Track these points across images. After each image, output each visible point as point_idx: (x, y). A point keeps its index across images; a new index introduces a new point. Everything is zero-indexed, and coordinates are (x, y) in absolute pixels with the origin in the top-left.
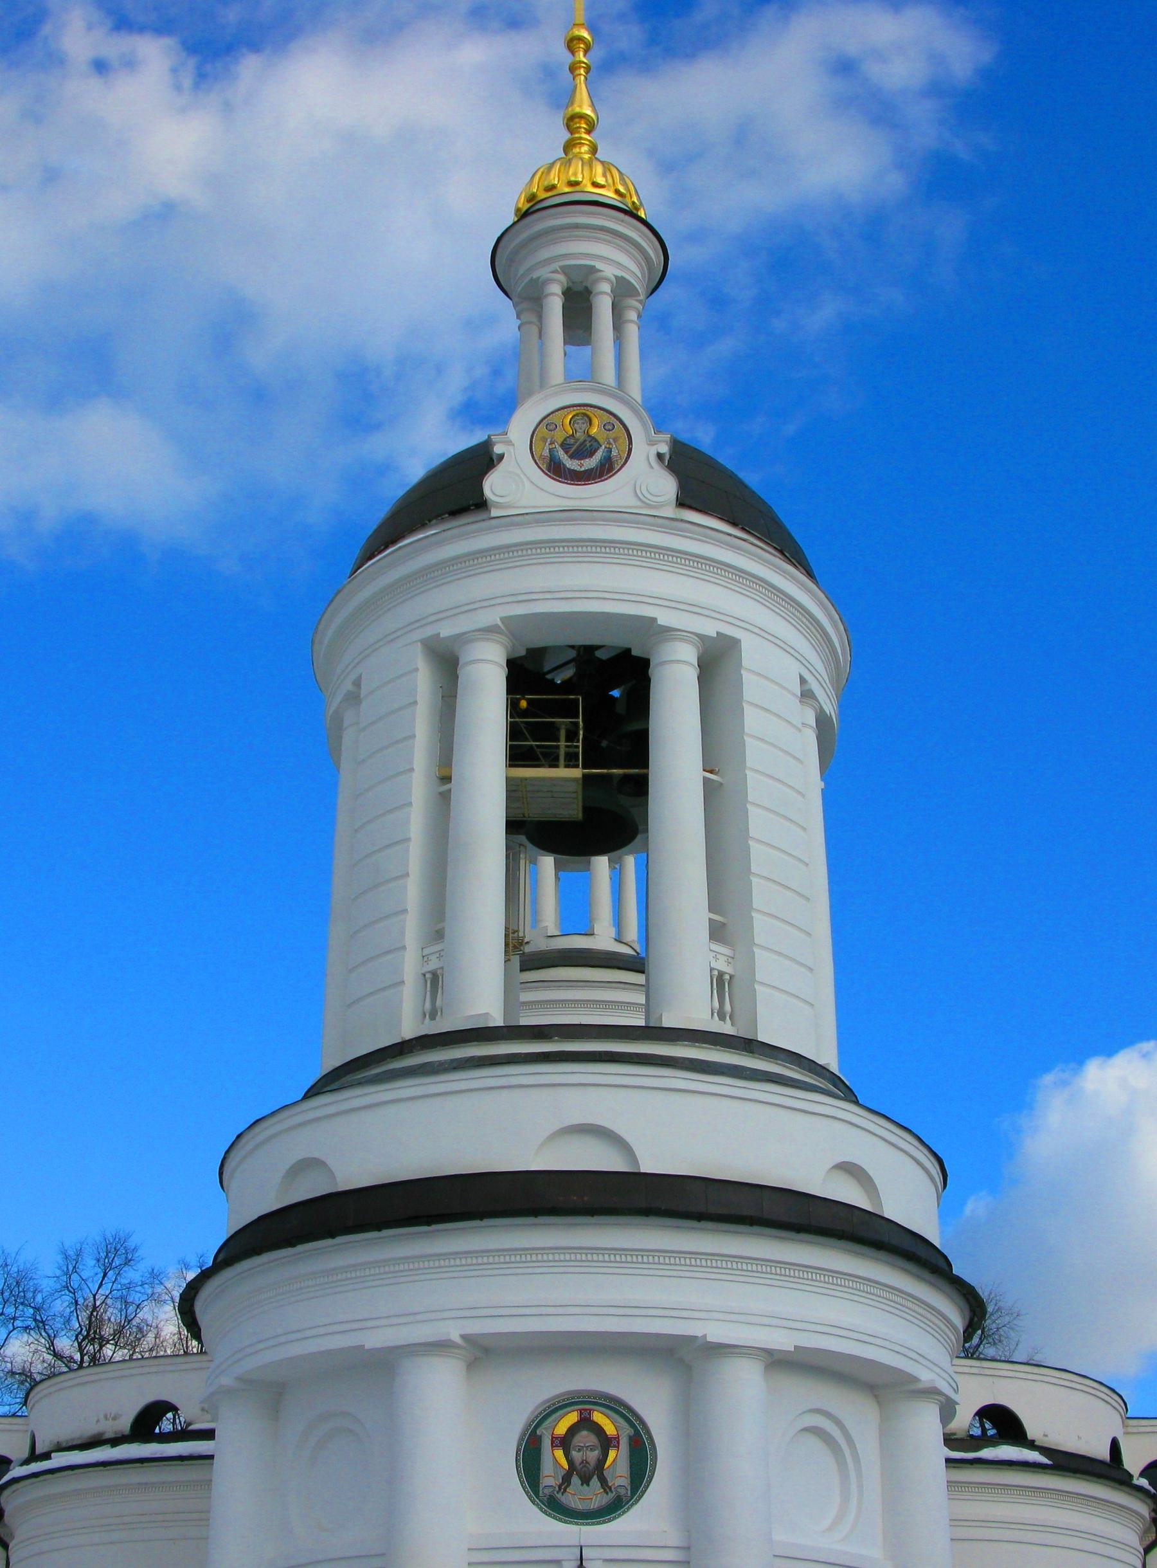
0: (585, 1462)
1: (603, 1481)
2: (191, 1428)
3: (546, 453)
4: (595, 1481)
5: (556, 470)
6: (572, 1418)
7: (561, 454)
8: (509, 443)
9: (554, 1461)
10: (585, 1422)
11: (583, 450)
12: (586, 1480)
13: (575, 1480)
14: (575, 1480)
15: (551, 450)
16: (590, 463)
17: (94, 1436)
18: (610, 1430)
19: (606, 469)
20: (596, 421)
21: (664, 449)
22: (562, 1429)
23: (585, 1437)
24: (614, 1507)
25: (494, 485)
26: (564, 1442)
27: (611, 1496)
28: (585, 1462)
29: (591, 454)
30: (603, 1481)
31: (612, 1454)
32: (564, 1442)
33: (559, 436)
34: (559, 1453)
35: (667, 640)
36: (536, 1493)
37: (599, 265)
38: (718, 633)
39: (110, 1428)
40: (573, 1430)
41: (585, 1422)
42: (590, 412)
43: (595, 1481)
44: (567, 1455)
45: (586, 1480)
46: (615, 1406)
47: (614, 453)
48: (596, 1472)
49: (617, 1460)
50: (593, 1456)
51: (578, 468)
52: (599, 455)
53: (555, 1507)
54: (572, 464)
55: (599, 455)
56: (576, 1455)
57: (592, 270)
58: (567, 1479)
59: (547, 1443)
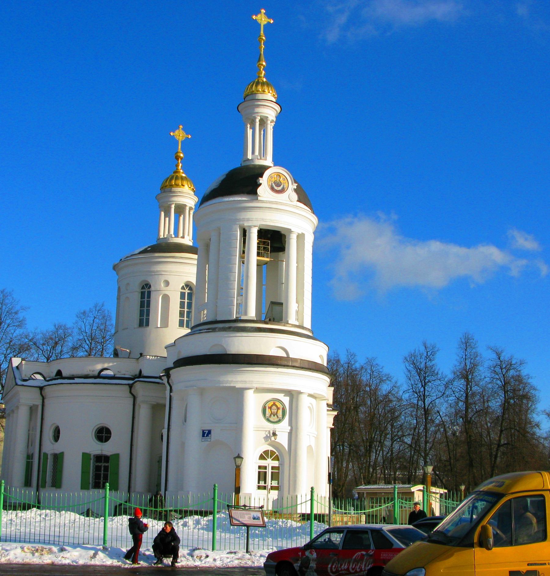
0: (274, 412)
1: (277, 416)
2: (115, 376)
3: (270, 184)
4: (276, 416)
5: (272, 189)
6: (272, 403)
7: (274, 185)
8: (263, 180)
9: (268, 412)
10: (274, 404)
11: (278, 185)
12: (274, 416)
13: (272, 415)
14: (272, 415)
15: (271, 183)
16: (280, 188)
17: (86, 375)
18: (279, 406)
19: (282, 191)
20: (281, 177)
21: (295, 188)
22: (270, 406)
23: (274, 407)
24: (279, 421)
25: (260, 190)
26: (270, 408)
27: (279, 419)
28: (274, 412)
29: (280, 186)
30: (277, 416)
31: (279, 410)
32: (270, 408)
33: (273, 180)
34: (269, 410)
35: (293, 233)
36: (265, 417)
37: (269, 117)
38: (302, 233)
39: (91, 374)
40: (272, 406)
41: (274, 404)
42: (281, 175)
43: (276, 416)
44: (271, 410)
45: (274, 416)
46: (280, 401)
47: (285, 187)
48: (276, 414)
49: (280, 412)
50: (276, 411)
51: (277, 189)
52: (282, 186)
53: (268, 420)
54: (276, 188)
55: (282, 186)
56: (273, 411)
57: (267, 117)
58: (271, 415)
59: (267, 408)
